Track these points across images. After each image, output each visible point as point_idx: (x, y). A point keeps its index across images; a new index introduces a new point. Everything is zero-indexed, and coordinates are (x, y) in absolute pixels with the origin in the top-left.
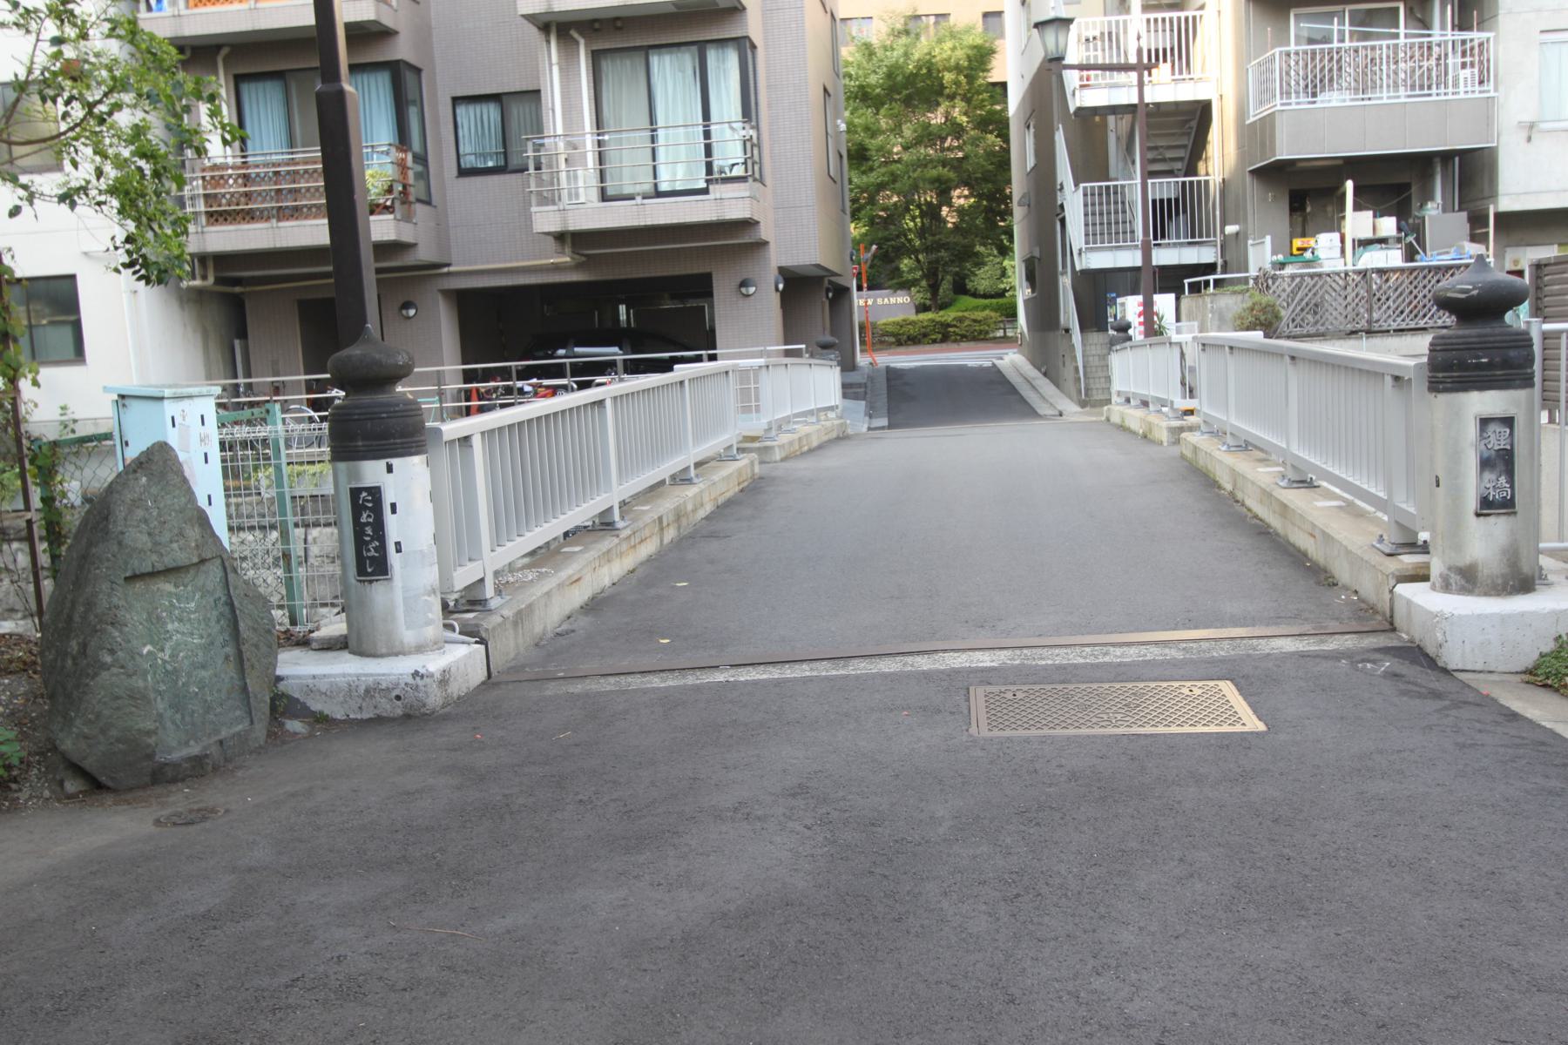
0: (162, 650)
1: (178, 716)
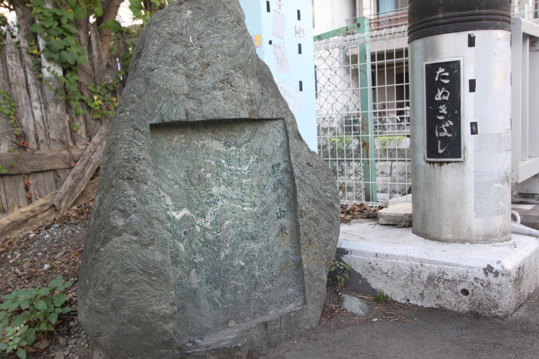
0: (203, 216)
1: (218, 293)
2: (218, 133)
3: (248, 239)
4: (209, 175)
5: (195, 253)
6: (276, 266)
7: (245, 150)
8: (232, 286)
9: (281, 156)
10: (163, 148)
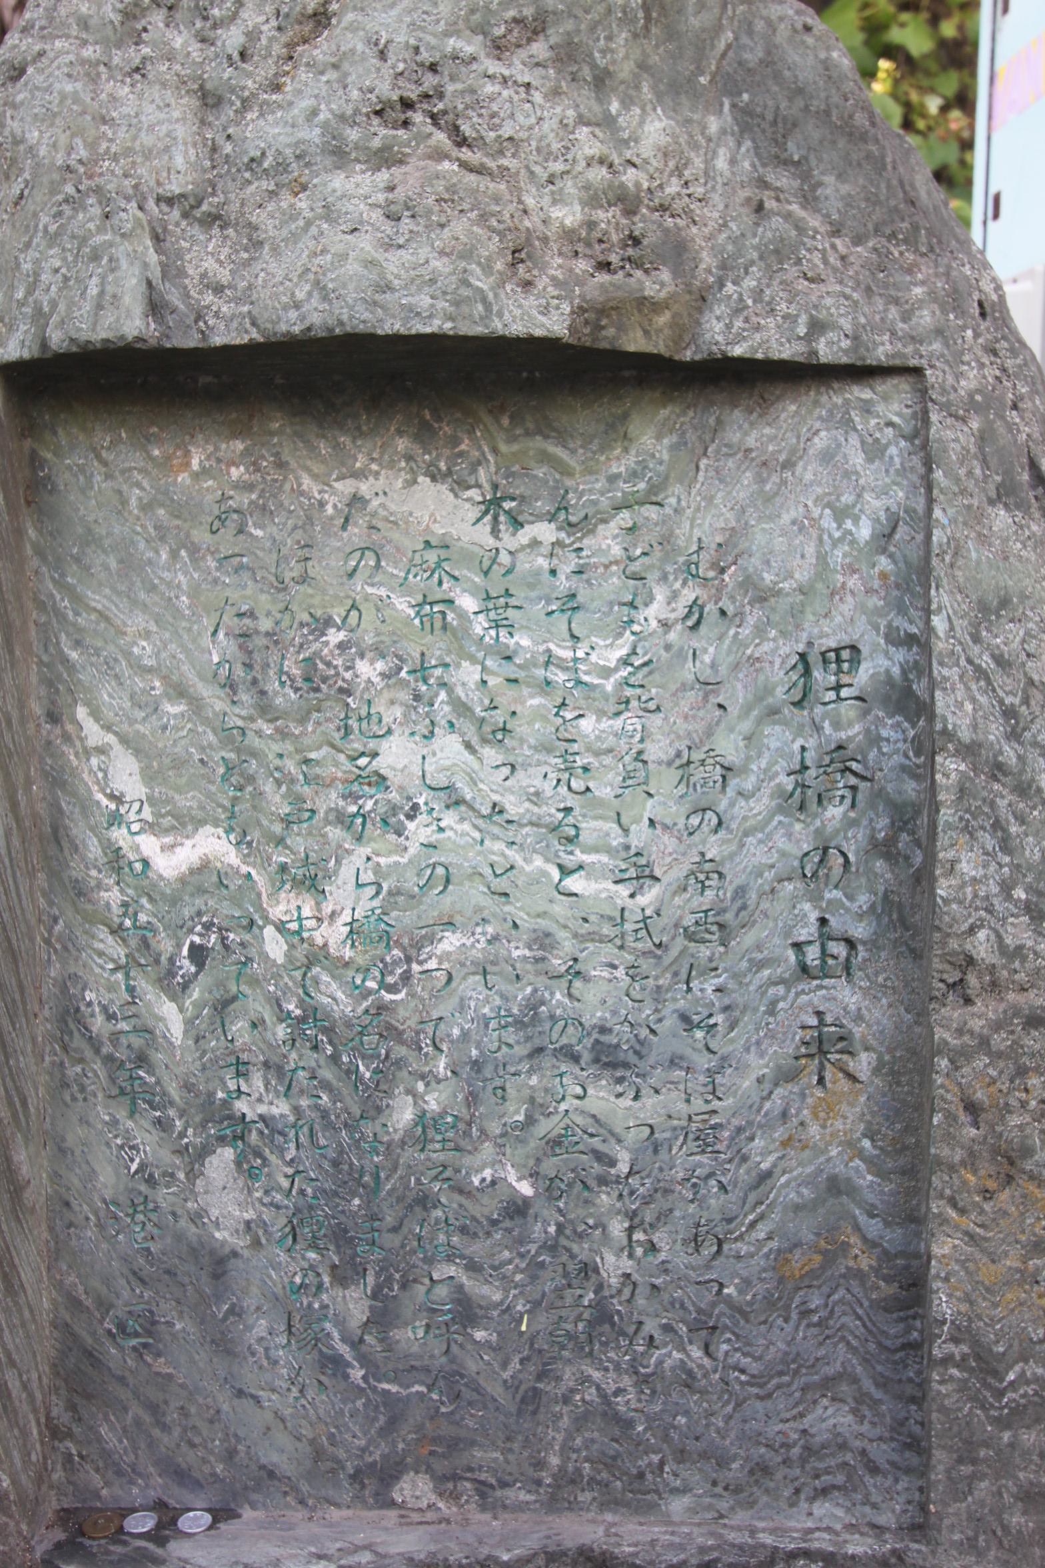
0: (311, 881)
1: (355, 1304)
2: (455, 441)
3: (576, 1059)
4: (368, 670)
5: (241, 1070)
6: (754, 1246)
7: (617, 551)
8: (442, 1291)
9: (875, 602)
10: (124, 502)
